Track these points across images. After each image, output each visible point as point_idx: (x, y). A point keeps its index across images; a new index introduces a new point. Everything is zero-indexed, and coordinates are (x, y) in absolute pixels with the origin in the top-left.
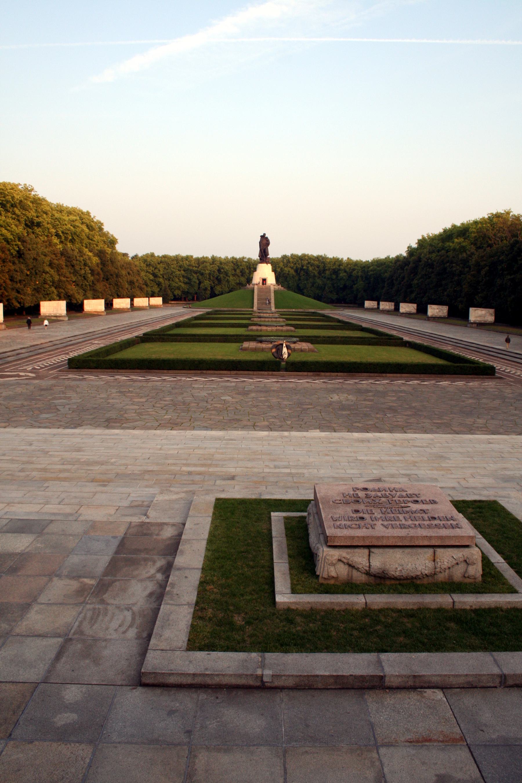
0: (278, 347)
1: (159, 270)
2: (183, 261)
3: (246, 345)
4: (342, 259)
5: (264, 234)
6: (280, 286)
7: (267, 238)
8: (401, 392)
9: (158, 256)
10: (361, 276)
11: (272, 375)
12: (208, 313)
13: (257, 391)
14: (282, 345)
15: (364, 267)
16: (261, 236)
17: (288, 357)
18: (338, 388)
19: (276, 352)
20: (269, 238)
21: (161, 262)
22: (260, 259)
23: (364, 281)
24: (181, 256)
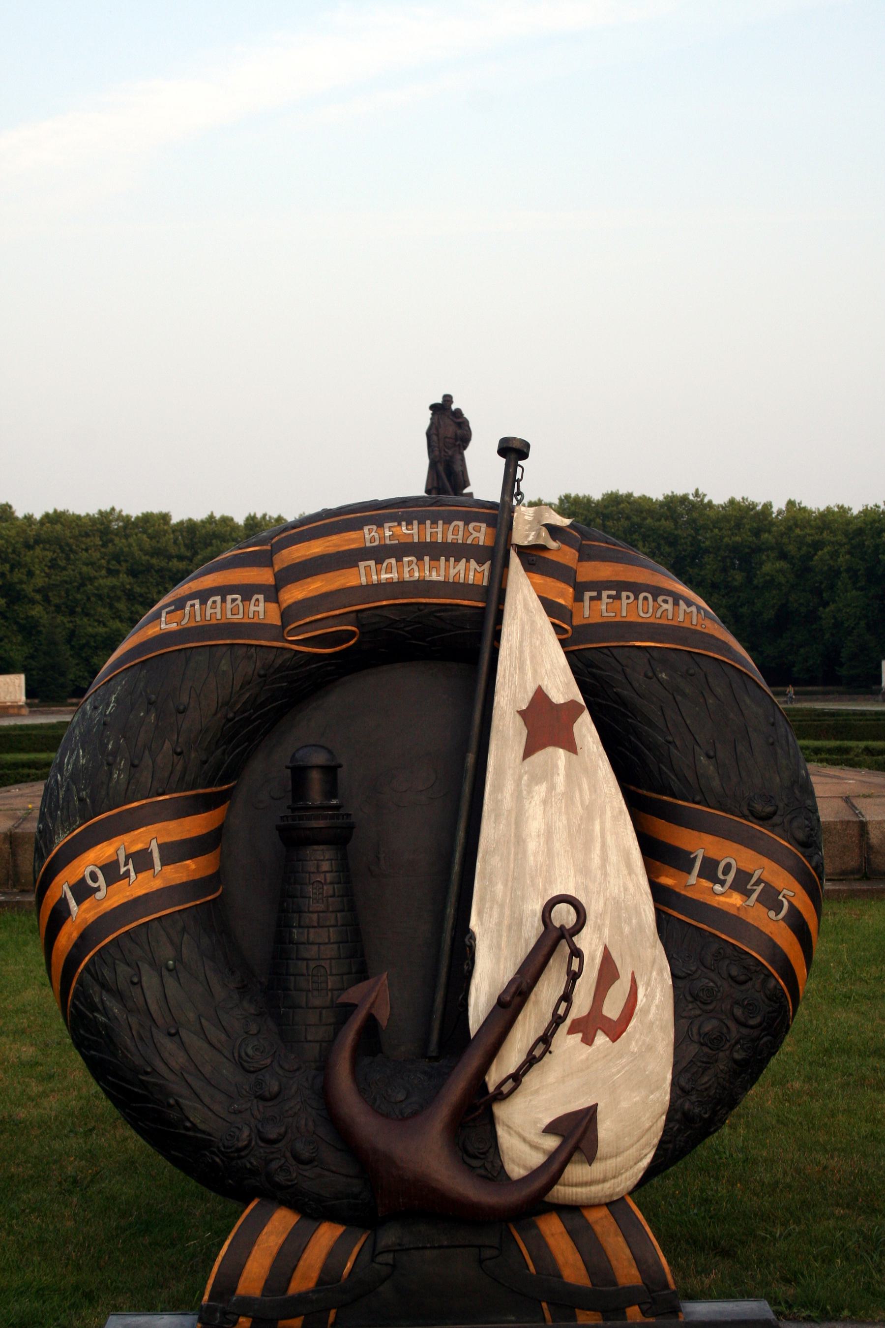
0: (312, 734)
1: (30, 574)
2: (127, 537)
4: (768, 506)
5: (448, 399)
7: (458, 413)
9: (29, 518)
10: (848, 570)
15: (860, 532)
16: (434, 408)
17: (688, 1127)
19: (207, 912)
20: (467, 414)
21: (38, 541)
23: (861, 589)
24: (120, 517)
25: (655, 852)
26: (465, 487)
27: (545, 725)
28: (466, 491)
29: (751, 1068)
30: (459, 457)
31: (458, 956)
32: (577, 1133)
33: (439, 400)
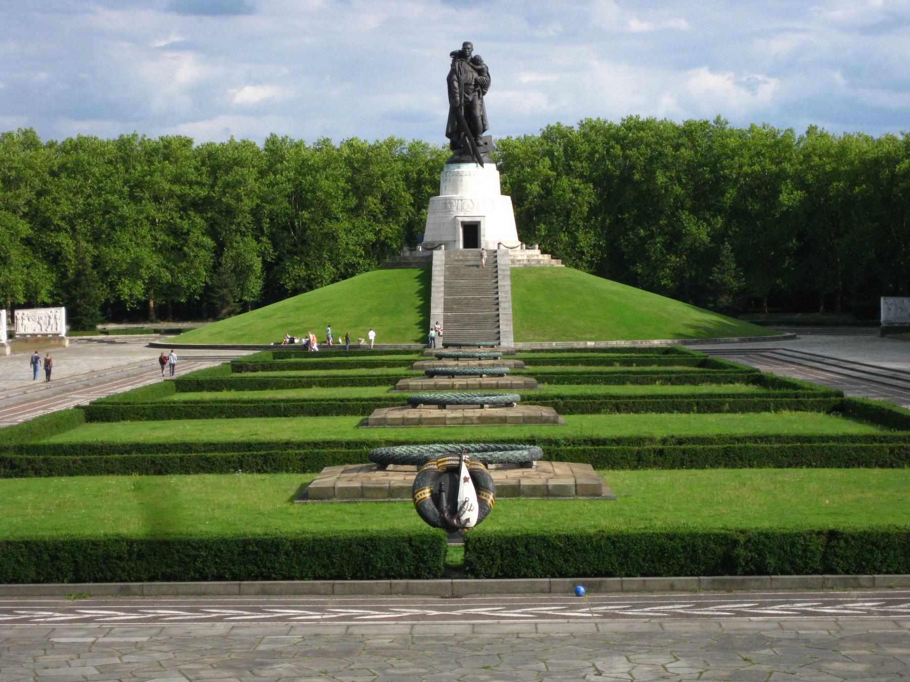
3: (330, 477)
6: (536, 253)
7: (476, 61)
8: (896, 640)
11: (407, 592)
12: (238, 366)
13: (305, 654)
14: (456, 470)
17: (479, 521)
18: (640, 635)
20: (487, 61)
22: (453, 146)
25: (478, 493)
26: (484, 130)
27: (466, 480)
28: (485, 134)
29: (487, 514)
30: (478, 102)
31: (457, 503)
32: (468, 520)
33: (459, 48)
